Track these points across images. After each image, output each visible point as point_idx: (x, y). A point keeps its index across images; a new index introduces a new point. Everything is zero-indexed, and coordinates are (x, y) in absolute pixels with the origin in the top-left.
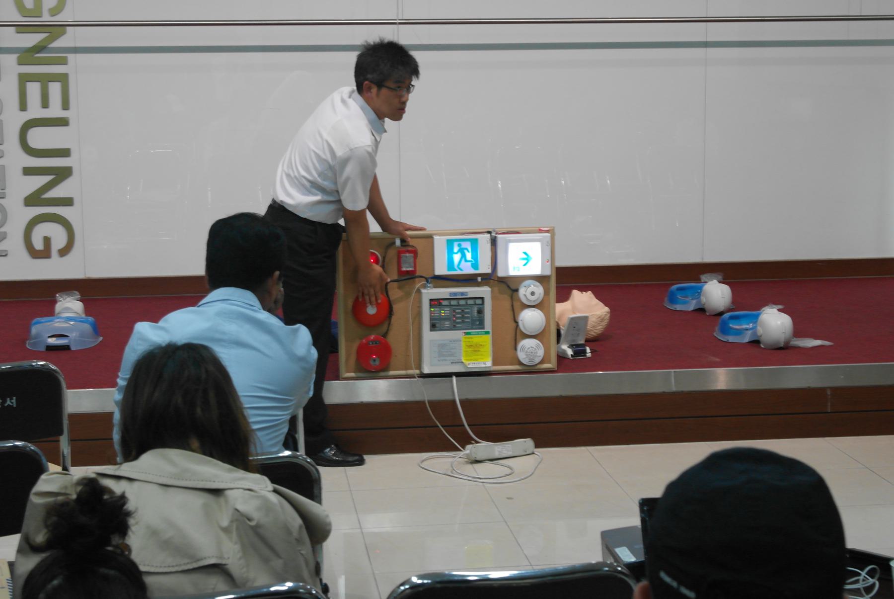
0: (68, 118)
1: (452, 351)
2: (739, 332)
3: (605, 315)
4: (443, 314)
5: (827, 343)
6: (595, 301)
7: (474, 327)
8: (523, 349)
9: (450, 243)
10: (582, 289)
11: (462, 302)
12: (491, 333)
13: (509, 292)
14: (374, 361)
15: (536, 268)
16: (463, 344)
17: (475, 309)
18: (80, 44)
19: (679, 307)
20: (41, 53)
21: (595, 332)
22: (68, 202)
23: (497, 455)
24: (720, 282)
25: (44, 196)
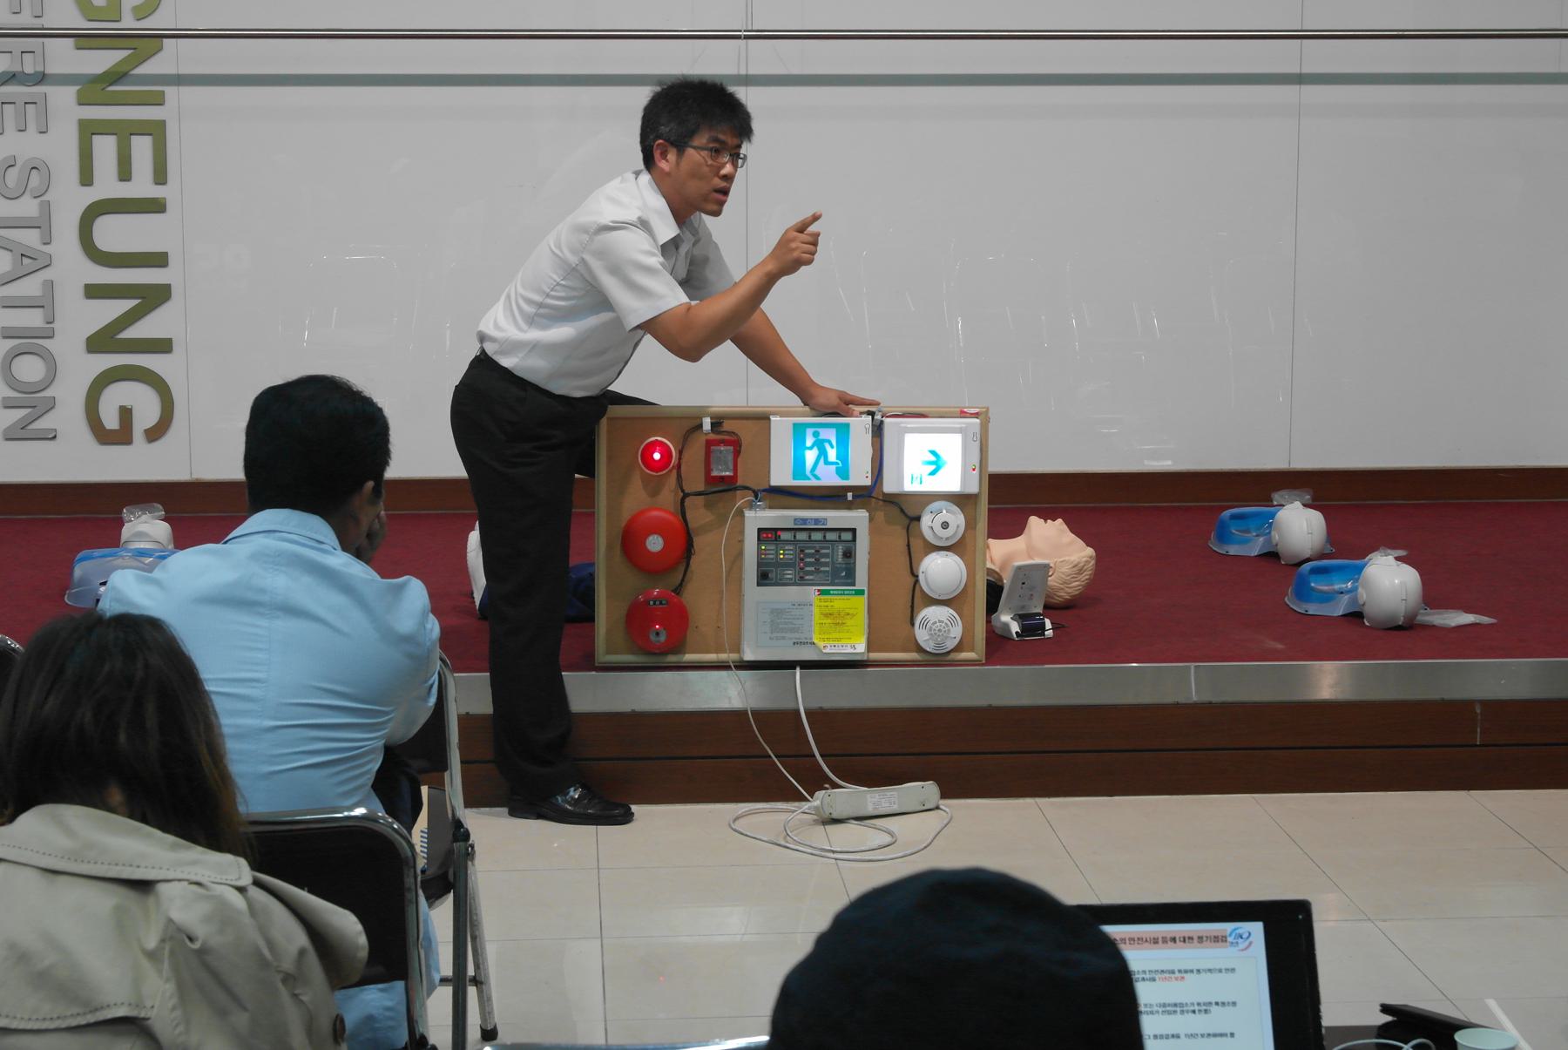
0: (165, 199)
1: (795, 622)
2: (1327, 597)
4: (782, 556)
5: (1485, 620)
6: (1069, 537)
7: (836, 581)
8: (924, 624)
9: (799, 430)
10: (1047, 515)
11: (817, 536)
12: (866, 592)
13: (907, 521)
14: (658, 634)
15: (951, 480)
16: (816, 611)
17: (840, 549)
18: (185, 70)
19: (1233, 550)
20: (116, 85)
22: (162, 346)
23: (870, 810)
24: (1305, 505)
25: (123, 335)
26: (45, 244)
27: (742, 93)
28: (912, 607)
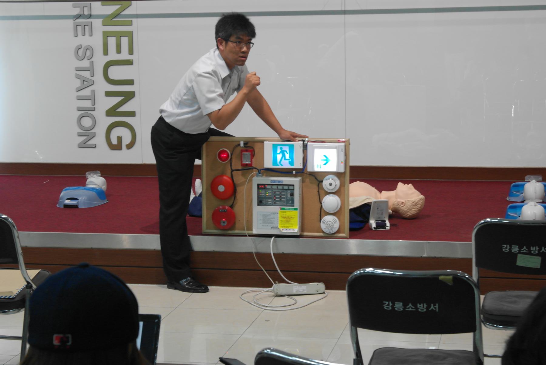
0: (133, 60)
1: (272, 220)
3: (418, 201)
4: (267, 195)
7: (288, 205)
8: (324, 222)
9: (275, 147)
10: (405, 182)
11: (280, 187)
14: (224, 223)
15: (333, 166)
16: (280, 216)
17: (289, 192)
20: (116, 18)
21: (410, 213)
22: (132, 114)
23: (294, 292)
26: (92, 76)
27: (253, 20)
28: (320, 215)
